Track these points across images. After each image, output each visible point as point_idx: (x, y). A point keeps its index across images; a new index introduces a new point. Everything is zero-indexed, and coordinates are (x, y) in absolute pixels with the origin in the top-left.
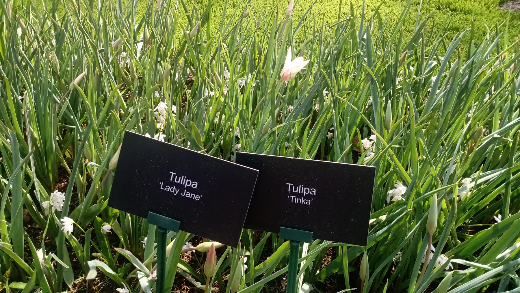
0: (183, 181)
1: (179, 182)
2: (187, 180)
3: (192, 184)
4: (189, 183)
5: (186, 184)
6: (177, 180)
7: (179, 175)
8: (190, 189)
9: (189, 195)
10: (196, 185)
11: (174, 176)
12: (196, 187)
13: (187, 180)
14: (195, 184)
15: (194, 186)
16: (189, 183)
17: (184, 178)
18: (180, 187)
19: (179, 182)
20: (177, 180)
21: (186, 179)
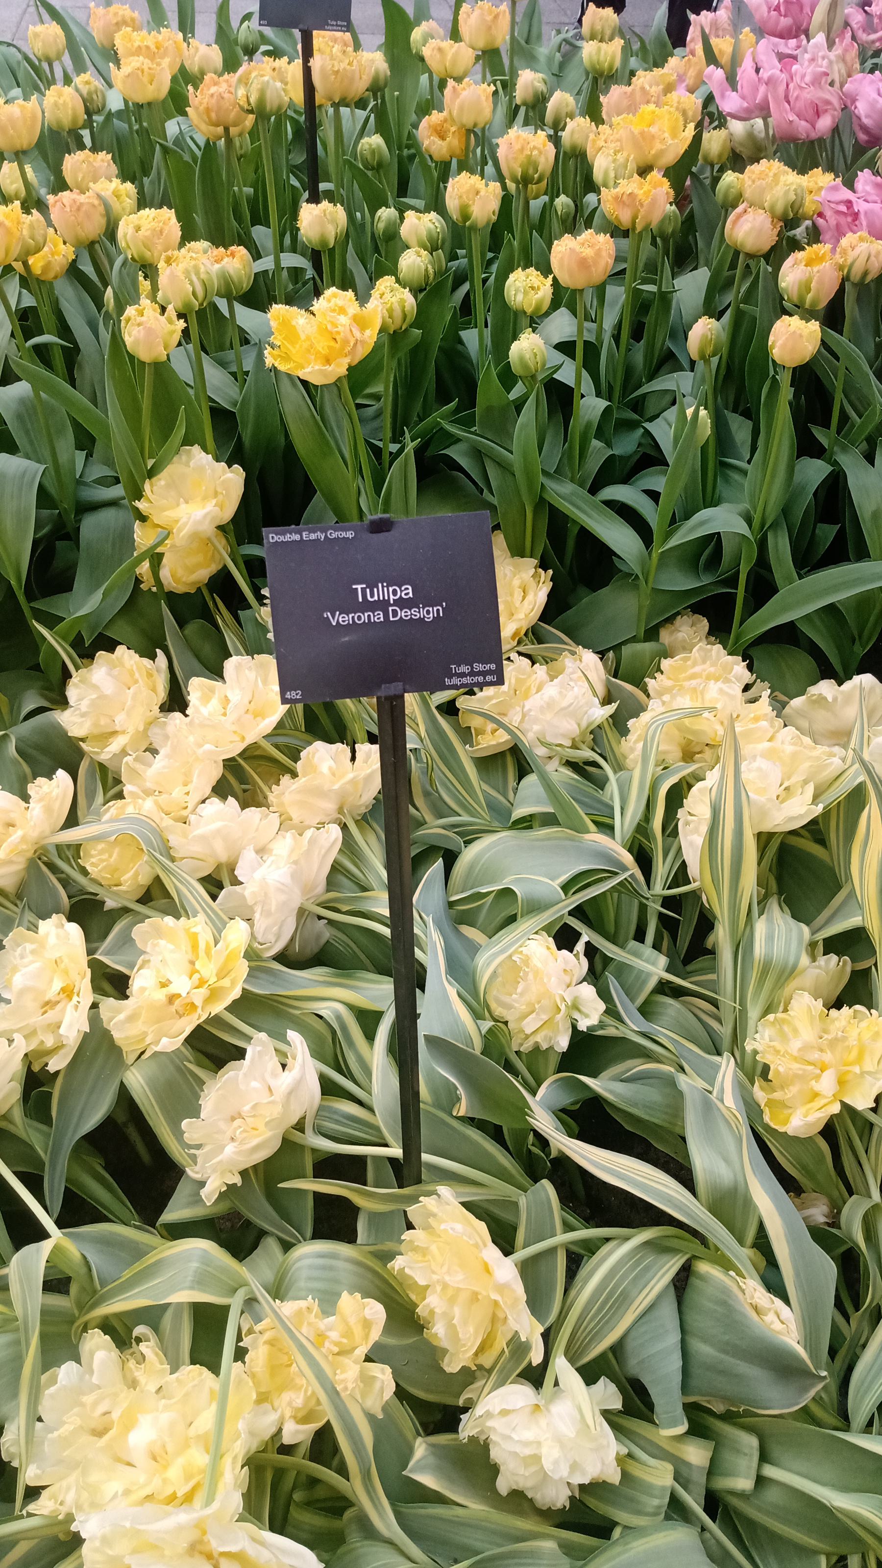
0: (381, 592)
1: (376, 598)
3: (401, 591)
5: (392, 597)
6: (372, 596)
7: (372, 586)
8: (402, 603)
9: (403, 614)
10: (410, 591)
12: (411, 595)
13: (391, 589)
14: (407, 589)
15: (406, 594)
17: (383, 587)
18: (383, 605)
19: (376, 598)
20: (372, 596)
21: (388, 587)
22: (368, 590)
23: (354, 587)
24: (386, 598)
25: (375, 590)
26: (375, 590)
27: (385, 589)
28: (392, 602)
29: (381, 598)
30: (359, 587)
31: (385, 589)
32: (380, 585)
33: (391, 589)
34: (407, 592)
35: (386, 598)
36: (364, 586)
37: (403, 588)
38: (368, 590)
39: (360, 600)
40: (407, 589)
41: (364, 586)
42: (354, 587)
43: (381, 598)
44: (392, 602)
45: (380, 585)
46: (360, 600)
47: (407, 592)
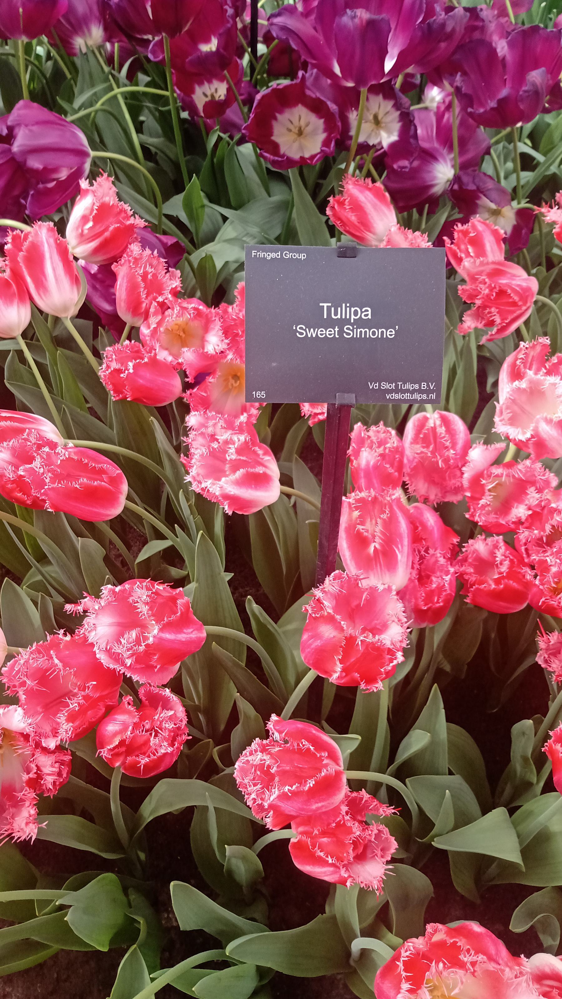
0: (346, 312)
1: (339, 316)
2: (353, 309)
3: (362, 312)
4: (356, 313)
5: (353, 317)
6: (336, 314)
8: (360, 323)
10: (369, 313)
11: (329, 308)
12: (370, 317)
14: (368, 311)
16: (356, 313)
17: (346, 307)
19: (339, 316)
20: (336, 314)
22: (333, 309)
23: (321, 304)
24: (348, 317)
25: (339, 309)
26: (339, 309)
27: (348, 309)
28: (352, 321)
29: (344, 317)
30: (325, 305)
31: (348, 309)
32: (344, 305)
33: (353, 309)
34: (367, 313)
35: (348, 317)
36: (330, 304)
37: (363, 310)
38: (333, 309)
39: (325, 317)
40: (368, 311)
41: (330, 304)
42: (321, 304)
43: (344, 317)
44: (352, 321)
45: (344, 305)
46: (325, 317)
47: (367, 313)
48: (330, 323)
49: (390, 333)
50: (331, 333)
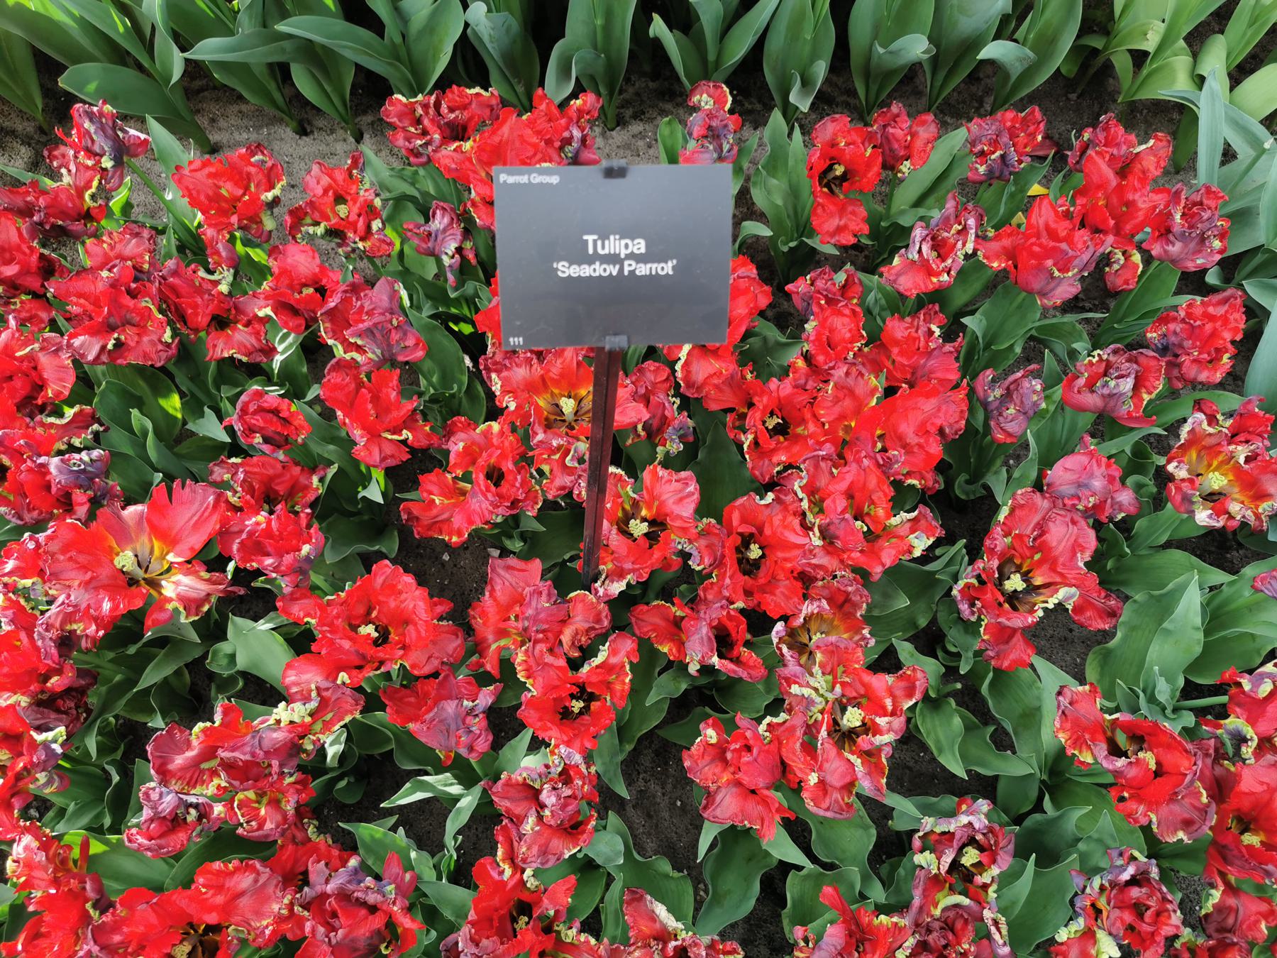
0: (615, 245)
2: (623, 242)
4: (627, 246)
6: (603, 248)
7: (604, 237)
11: (595, 242)
12: (643, 250)
16: (627, 246)
19: (606, 251)
20: (603, 248)
22: (599, 243)
23: (585, 237)
25: (607, 242)
30: (590, 238)
32: (612, 237)
34: (640, 246)
38: (599, 243)
39: (591, 251)
41: (595, 237)
42: (585, 237)
46: (591, 251)
47: (640, 246)
48: (596, 258)
49: (667, 268)
50: (598, 270)
